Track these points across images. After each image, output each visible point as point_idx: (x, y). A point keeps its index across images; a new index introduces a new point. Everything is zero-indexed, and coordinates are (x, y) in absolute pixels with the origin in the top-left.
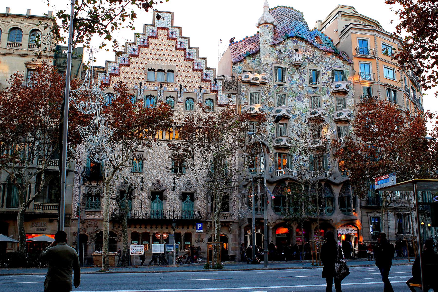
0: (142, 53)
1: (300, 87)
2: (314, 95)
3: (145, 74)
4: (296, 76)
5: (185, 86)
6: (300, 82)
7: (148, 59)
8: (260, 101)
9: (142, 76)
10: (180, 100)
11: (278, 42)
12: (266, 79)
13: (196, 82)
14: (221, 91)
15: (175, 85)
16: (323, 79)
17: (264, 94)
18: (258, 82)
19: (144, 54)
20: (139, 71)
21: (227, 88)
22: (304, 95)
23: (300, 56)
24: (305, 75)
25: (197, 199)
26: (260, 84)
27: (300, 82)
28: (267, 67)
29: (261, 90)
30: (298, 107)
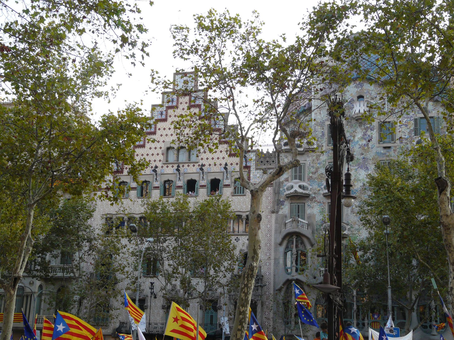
0: (159, 129)
1: (364, 149)
2: (384, 158)
3: (163, 154)
4: (359, 135)
5: (210, 165)
6: (364, 142)
7: (167, 135)
8: (306, 175)
9: (158, 158)
10: (203, 183)
11: (332, 90)
12: (314, 144)
13: (224, 158)
14: (254, 167)
15: (197, 164)
16: (401, 133)
17: (312, 165)
18: (301, 149)
19: (162, 129)
20: (155, 152)
21: (262, 162)
22: (370, 159)
23: (362, 105)
24: (372, 132)
25: (220, 308)
26: (306, 151)
27: (364, 142)
28: (317, 127)
29: (308, 159)
30: (361, 178)
